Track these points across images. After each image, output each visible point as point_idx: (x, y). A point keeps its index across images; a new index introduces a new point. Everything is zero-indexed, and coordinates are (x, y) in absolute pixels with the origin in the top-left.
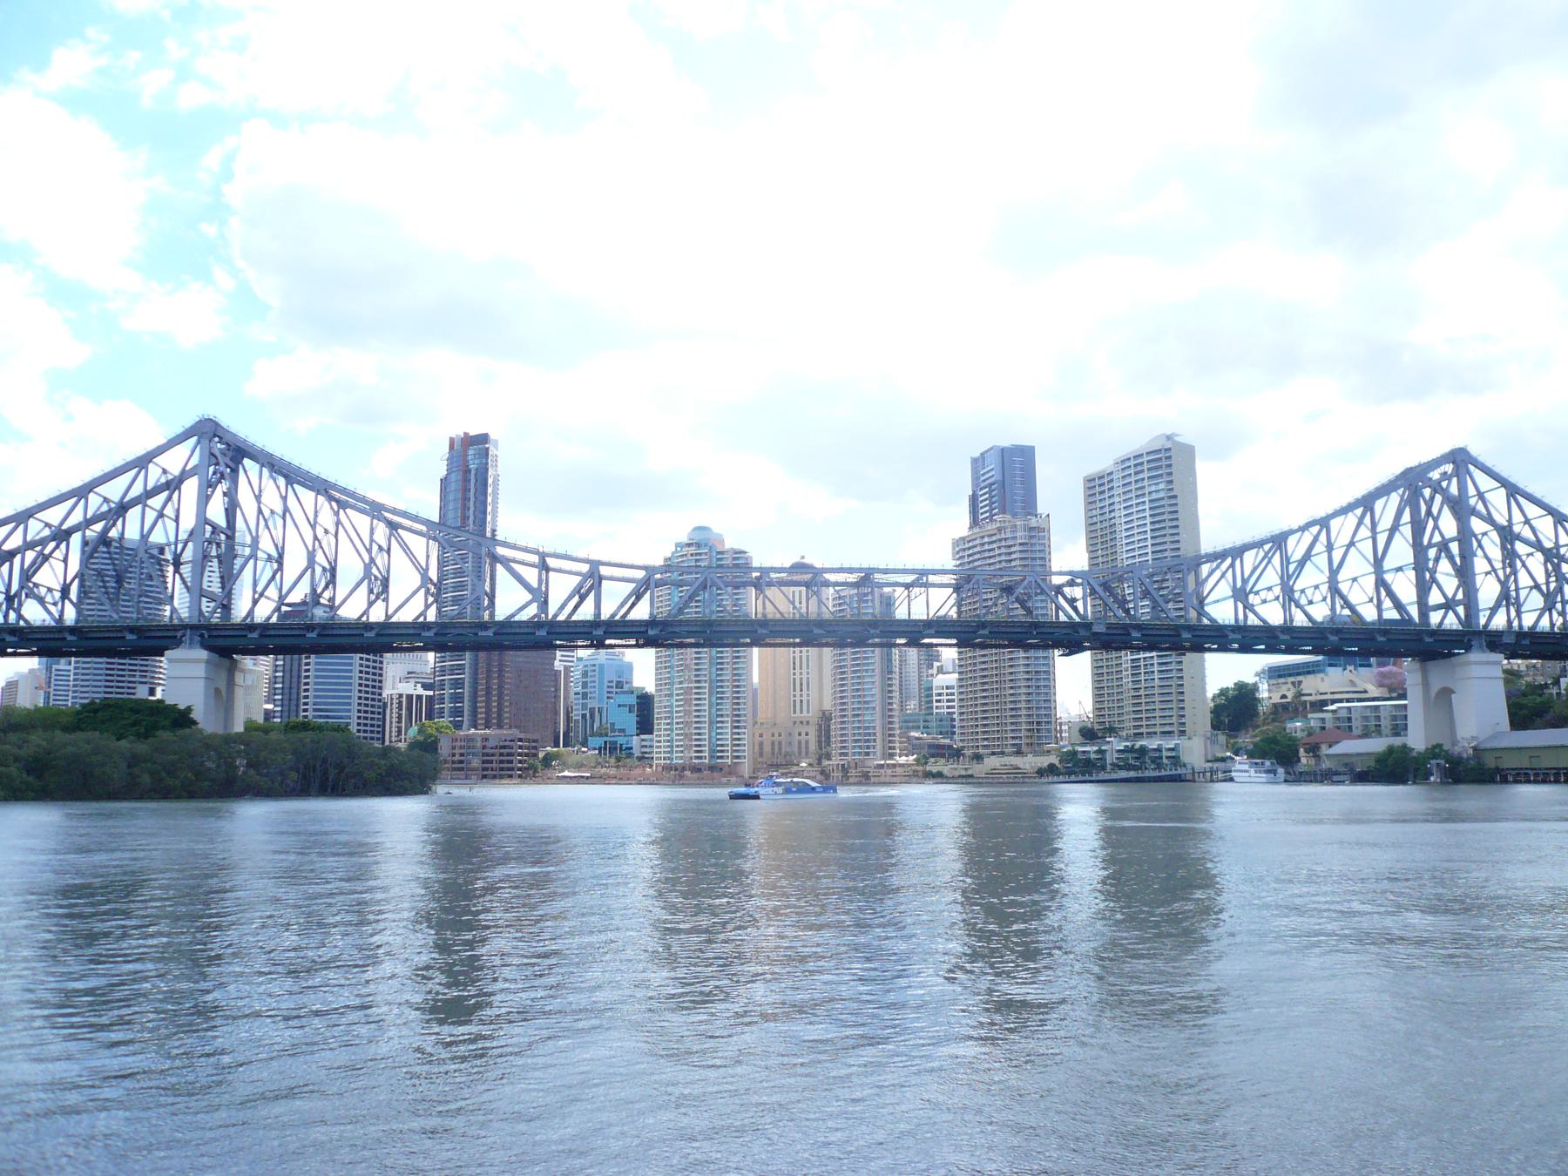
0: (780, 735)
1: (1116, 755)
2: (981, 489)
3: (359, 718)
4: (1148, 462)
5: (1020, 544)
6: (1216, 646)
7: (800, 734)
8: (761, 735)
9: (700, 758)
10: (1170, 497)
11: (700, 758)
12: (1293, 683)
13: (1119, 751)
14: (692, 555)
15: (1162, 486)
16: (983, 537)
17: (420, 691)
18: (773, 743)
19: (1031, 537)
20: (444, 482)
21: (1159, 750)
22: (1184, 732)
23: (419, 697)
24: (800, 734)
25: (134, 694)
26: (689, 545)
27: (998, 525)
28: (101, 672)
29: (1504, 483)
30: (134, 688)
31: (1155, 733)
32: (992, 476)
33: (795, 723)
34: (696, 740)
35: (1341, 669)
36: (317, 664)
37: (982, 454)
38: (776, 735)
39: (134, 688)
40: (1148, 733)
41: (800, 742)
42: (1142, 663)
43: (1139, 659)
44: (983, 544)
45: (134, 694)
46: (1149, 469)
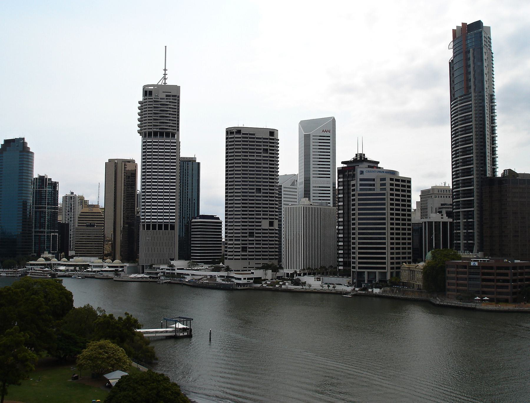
3: (392, 244)
17: (446, 219)
20: (451, 64)
23: (445, 224)
25: (260, 226)
28: (239, 209)
30: (260, 222)
39: (260, 222)
45: (260, 226)
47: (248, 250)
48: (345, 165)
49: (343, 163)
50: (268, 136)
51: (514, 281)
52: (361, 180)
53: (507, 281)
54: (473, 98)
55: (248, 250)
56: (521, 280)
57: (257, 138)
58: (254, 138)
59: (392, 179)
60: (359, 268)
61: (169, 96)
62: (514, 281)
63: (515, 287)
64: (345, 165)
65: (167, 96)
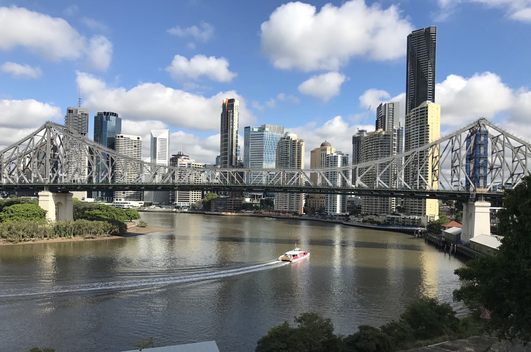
0: (315, 201)
1: (402, 220)
2: (379, 118)
4: (420, 112)
5: (381, 141)
7: (321, 202)
8: (310, 201)
9: (286, 209)
11: (286, 209)
13: (403, 218)
14: (285, 142)
16: (370, 138)
18: (313, 204)
24: (321, 202)
26: (284, 138)
31: (416, 213)
32: (382, 114)
33: (321, 197)
34: (285, 203)
38: (314, 201)
39: (132, 180)
40: (415, 213)
41: (321, 204)
44: (370, 140)
46: (420, 115)
47: (126, 193)
48: (174, 157)
49: (172, 155)
50: (136, 139)
51: (234, 205)
52: (180, 164)
53: (232, 205)
54: (229, 132)
55: (126, 193)
56: (237, 205)
57: (131, 140)
58: (129, 140)
59: (193, 165)
60: (178, 201)
61: (83, 114)
62: (234, 205)
63: (234, 207)
64: (174, 157)
65: (82, 114)
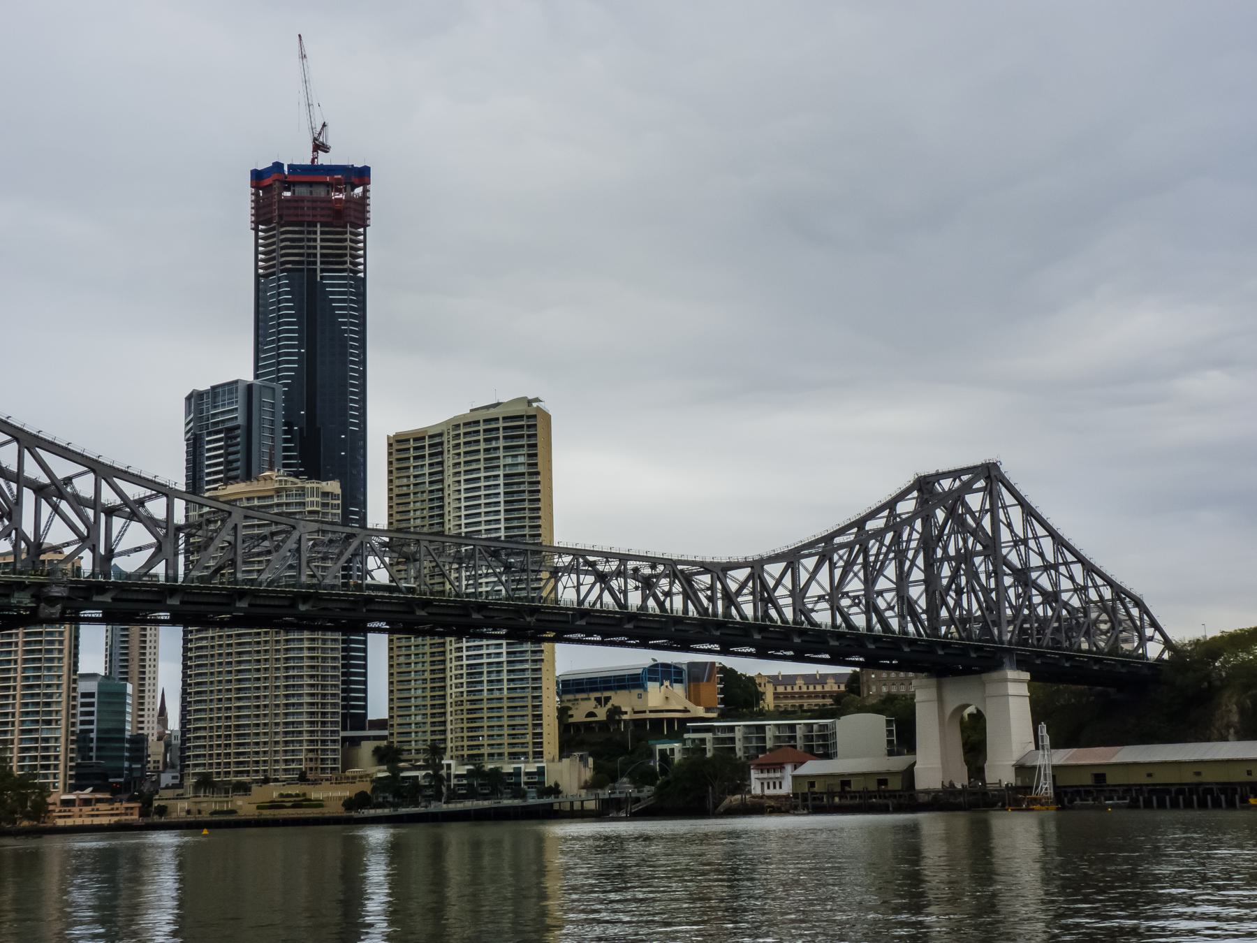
2: (209, 434)
4: (505, 428)
6: (791, 653)
10: (531, 474)
12: (598, 700)
15: (521, 460)
19: (325, 505)
21: (517, 773)
22: (541, 753)
27: (277, 486)
29: (1022, 502)
35: (658, 684)
36: (468, 648)
37: (214, 388)
42: (485, 669)
43: (482, 664)
